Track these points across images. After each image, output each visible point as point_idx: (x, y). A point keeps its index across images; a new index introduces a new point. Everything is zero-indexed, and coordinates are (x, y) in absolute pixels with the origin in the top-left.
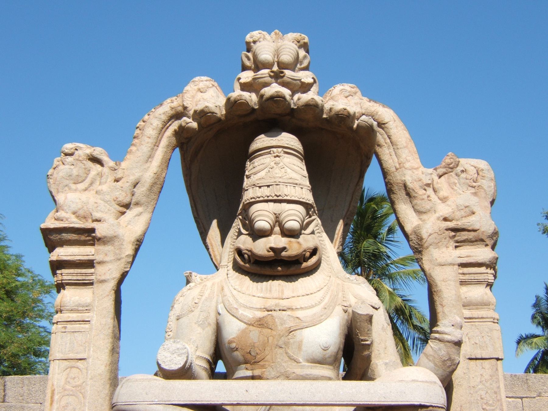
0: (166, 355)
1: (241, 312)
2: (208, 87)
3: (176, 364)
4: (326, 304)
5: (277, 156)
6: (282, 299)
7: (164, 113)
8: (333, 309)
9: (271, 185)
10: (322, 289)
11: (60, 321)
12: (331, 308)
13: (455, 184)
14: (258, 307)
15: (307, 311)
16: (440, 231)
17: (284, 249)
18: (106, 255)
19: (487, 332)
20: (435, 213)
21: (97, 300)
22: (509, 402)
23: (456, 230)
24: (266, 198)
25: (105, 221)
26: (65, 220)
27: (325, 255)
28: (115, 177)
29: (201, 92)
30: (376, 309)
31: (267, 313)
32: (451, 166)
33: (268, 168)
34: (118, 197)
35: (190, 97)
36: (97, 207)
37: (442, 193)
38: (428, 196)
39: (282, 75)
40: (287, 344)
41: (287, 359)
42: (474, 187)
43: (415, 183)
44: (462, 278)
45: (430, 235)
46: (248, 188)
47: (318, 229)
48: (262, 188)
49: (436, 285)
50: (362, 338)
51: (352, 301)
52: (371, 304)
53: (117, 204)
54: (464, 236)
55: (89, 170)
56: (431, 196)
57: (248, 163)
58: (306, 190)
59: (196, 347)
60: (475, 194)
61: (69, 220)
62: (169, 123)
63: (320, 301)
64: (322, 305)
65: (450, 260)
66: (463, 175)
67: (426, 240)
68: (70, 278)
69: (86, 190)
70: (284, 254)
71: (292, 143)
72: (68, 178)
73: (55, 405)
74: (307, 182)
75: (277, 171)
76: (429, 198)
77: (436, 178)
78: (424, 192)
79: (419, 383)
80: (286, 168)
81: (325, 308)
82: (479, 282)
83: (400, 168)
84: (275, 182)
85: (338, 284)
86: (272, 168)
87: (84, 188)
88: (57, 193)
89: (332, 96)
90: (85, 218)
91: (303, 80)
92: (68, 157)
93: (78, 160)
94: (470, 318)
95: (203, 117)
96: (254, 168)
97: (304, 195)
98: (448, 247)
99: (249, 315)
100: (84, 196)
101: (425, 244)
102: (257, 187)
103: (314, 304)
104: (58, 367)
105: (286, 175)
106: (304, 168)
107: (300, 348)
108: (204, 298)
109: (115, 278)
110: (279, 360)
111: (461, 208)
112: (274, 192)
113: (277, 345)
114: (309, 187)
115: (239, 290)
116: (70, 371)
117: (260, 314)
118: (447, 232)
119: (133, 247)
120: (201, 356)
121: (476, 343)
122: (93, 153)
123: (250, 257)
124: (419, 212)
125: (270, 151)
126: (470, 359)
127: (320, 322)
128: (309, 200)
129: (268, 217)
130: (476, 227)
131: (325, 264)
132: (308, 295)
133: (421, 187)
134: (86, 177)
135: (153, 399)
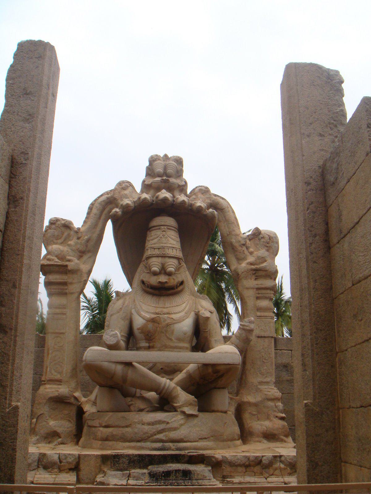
0: (108, 337)
1: (143, 313)
2: (128, 187)
3: (113, 342)
4: (186, 311)
5: (164, 231)
7: (103, 201)
8: (191, 313)
9: (160, 248)
12: (189, 313)
13: (258, 244)
15: (177, 314)
17: (166, 282)
18: (73, 279)
19: (268, 324)
20: (246, 259)
22: (285, 353)
23: (256, 270)
24: (157, 255)
27: (187, 284)
29: (124, 189)
30: (211, 312)
31: (155, 316)
32: (256, 234)
34: (79, 247)
36: (68, 253)
37: (251, 250)
38: (244, 251)
39: (168, 181)
40: (166, 331)
42: (267, 247)
44: (257, 295)
45: (242, 273)
49: (244, 299)
51: (200, 308)
53: (79, 252)
54: (260, 273)
55: (64, 232)
57: (148, 233)
60: (268, 251)
61: (54, 260)
62: (106, 206)
64: (186, 310)
65: (252, 286)
66: (263, 240)
69: (62, 243)
70: (166, 285)
71: (172, 224)
73: (50, 356)
74: (178, 245)
75: (164, 239)
77: (248, 241)
79: (228, 354)
80: (168, 238)
81: (186, 313)
82: (266, 298)
83: (229, 234)
84: (162, 246)
85: (193, 299)
87: (61, 242)
88: (47, 245)
90: (62, 259)
91: (179, 184)
94: (260, 316)
96: (151, 236)
99: (148, 316)
100: (61, 247)
103: (180, 311)
106: (178, 236)
107: (173, 333)
108: (125, 306)
109: (78, 292)
111: (260, 258)
114: (180, 249)
115: (142, 302)
117: (153, 316)
118: (251, 272)
119: (87, 276)
125: (160, 228)
126: (258, 337)
127: (184, 320)
129: (158, 265)
130: (267, 269)
131: (187, 288)
132: (177, 306)
133: (240, 246)
134: (62, 237)
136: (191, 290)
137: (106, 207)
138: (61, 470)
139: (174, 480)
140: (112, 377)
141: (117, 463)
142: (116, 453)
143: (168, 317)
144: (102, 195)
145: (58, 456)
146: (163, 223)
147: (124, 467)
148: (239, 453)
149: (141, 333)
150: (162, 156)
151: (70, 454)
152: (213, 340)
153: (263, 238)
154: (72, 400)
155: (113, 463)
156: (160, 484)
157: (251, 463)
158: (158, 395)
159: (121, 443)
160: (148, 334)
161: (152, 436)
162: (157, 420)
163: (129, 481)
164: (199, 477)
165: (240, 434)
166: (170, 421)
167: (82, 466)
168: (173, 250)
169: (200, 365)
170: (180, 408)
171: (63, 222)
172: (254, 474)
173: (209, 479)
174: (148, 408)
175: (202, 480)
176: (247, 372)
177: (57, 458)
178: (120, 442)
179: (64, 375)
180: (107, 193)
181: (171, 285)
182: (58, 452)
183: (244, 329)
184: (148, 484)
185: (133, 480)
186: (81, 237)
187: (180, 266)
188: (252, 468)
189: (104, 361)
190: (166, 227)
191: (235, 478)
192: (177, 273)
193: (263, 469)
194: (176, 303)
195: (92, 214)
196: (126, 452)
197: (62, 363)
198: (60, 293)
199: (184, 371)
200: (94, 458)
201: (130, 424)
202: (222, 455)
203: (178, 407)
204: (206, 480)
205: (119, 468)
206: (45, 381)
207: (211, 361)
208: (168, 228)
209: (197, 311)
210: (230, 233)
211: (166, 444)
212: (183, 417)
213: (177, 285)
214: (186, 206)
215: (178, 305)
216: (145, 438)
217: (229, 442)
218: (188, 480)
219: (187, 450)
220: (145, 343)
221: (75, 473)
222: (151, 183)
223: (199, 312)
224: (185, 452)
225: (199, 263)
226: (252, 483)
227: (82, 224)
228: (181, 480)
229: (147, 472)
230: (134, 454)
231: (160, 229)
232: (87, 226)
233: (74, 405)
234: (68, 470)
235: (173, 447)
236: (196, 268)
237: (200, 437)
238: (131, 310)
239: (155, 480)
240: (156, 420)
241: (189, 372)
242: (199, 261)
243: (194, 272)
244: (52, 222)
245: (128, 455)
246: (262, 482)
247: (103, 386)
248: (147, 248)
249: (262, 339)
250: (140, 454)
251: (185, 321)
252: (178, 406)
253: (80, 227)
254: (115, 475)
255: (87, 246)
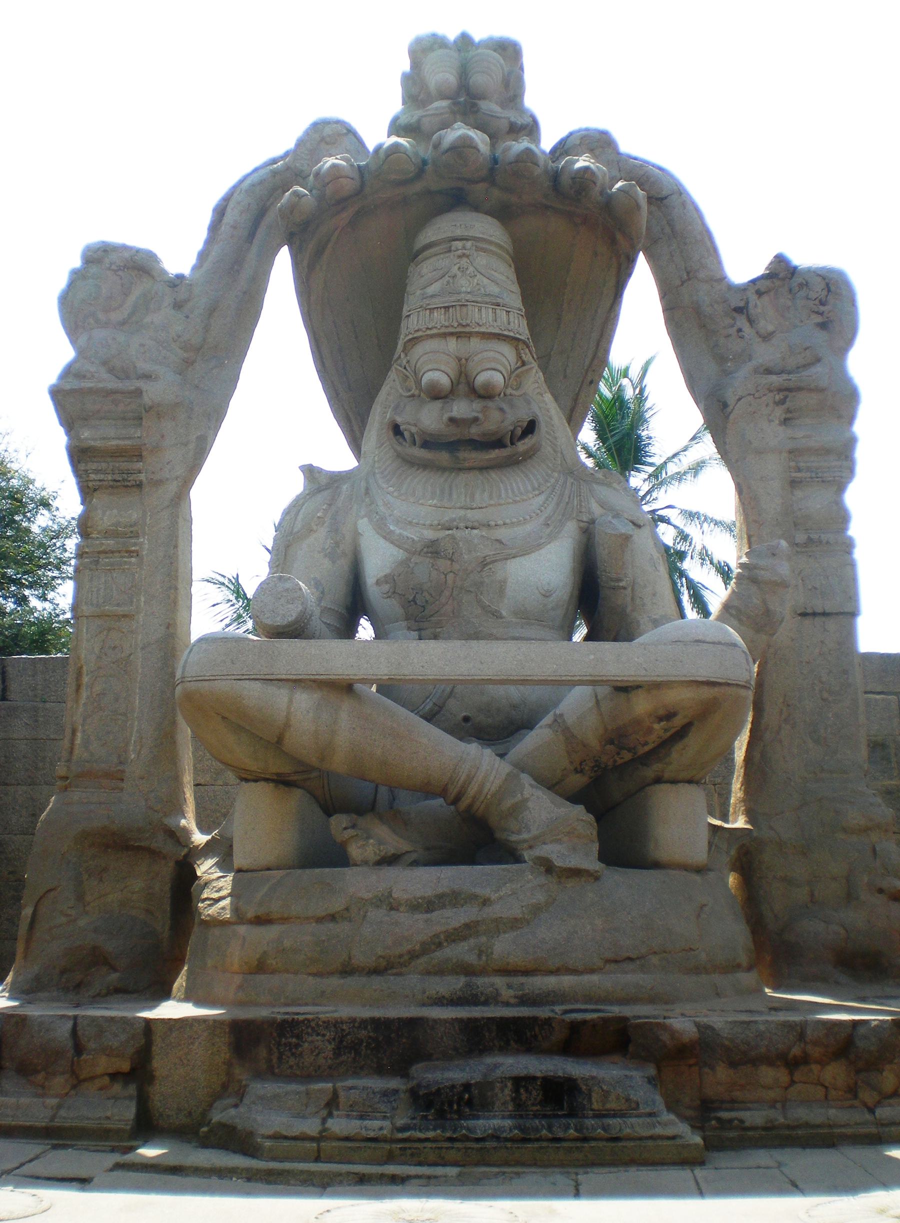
2: (339, 135)
4: (549, 518)
5: (464, 255)
6: (472, 509)
9: (453, 306)
10: (543, 492)
11: (87, 550)
14: (428, 522)
16: (758, 391)
17: (476, 420)
20: (750, 360)
21: (150, 515)
24: (443, 330)
25: (157, 378)
26: (88, 375)
28: (175, 299)
29: (327, 143)
30: (639, 526)
33: (447, 276)
35: (306, 152)
37: (765, 325)
38: (740, 330)
39: (475, 109)
41: (480, 611)
42: (822, 314)
43: (716, 306)
44: (794, 475)
45: (739, 399)
46: (410, 313)
47: (537, 388)
48: (435, 311)
50: (614, 576)
52: (630, 518)
56: (743, 329)
57: (410, 269)
58: (516, 315)
59: (323, 593)
63: (539, 511)
67: (731, 407)
68: (102, 477)
70: (474, 432)
72: (92, 302)
73: (84, 694)
76: (740, 334)
77: (753, 298)
78: (732, 322)
79: (705, 646)
81: (548, 524)
83: (689, 279)
84: (459, 301)
86: (454, 277)
89: (566, 147)
91: (513, 119)
92: (90, 264)
93: (109, 269)
95: (330, 185)
96: (422, 276)
97: (512, 324)
98: (773, 421)
101: (732, 414)
102: (426, 309)
104: (87, 629)
105: (479, 290)
106: (513, 277)
107: (501, 590)
109: (177, 478)
110: (465, 613)
112: (457, 319)
113: (461, 588)
114: (520, 310)
115: (395, 494)
116: (107, 636)
117: (430, 535)
118: (771, 394)
120: (330, 609)
121: (815, 588)
122: (136, 257)
123: (416, 436)
124: (721, 360)
125: (450, 247)
126: (804, 615)
127: (539, 547)
128: (520, 332)
131: (549, 449)
132: (515, 502)
135: (244, 672)
136: (562, 453)
137: (268, 203)
138: (82, 1077)
139: (510, 1117)
140: (280, 740)
141: (293, 1054)
142: (287, 1013)
143: (482, 536)
144: (256, 170)
145: (70, 1024)
146: (458, 233)
147: (319, 1067)
148: (760, 1013)
149: (388, 595)
150: (452, 35)
151: (112, 1019)
152: (643, 620)
153: (805, 285)
154: (159, 842)
155: (276, 1054)
156: (455, 1131)
157: (809, 1048)
158: (452, 807)
159: (311, 978)
160: (415, 597)
161: (427, 948)
162: (447, 890)
163: (330, 1123)
164: (608, 1106)
165: (753, 947)
166: (494, 897)
167: (160, 1064)
168: (498, 311)
169: (603, 691)
170: (531, 847)
171: (126, 255)
172: (820, 1092)
173: (650, 1115)
174: (415, 851)
175: (623, 1116)
176: (768, 736)
177: (67, 1035)
178: (310, 974)
179: (133, 756)
180: (274, 161)
181: (491, 428)
182: (71, 1013)
183: (754, 581)
184: (406, 1135)
185: (348, 1116)
186: (189, 300)
187: (525, 368)
188: (815, 1068)
189: (248, 679)
190: (469, 244)
191: (749, 1109)
192: (514, 392)
193: (858, 1071)
194: (513, 492)
195: (223, 228)
196: (326, 1013)
197: (125, 714)
198: (119, 484)
199: (548, 719)
200: (205, 1034)
201: (347, 909)
202: (697, 1019)
203: (525, 845)
204: (638, 1116)
205: (298, 1072)
206: (67, 778)
207: (643, 673)
208: (476, 247)
209: (585, 519)
210: (690, 275)
211: (481, 981)
212: (542, 880)
213: (512, 432)
214: (538, 171)
215: (518, 499)
216: (402, 960)
217: (717, 978)
218: (564, 1116)
219: (562, 1004)
220: (405, 631)
221: (132, 1089)
222: (419, 121)
223: (592, 522)
224: (553, 1011)
225: (589, 379)
226: (819, 1126)
227: (192, 260)
228: (535, 1116)
229: (403, 1087)
230: (353, 1020)
231: (450, 251)
232: (207, 265)
233: (165, 858)
234: (106, 1080)
235: (507, 994)
236: (578, 394)
237: (609, 955)
238: (355, 525)
239: (435, 1119)
240: (440, 890)
241: (564, 721)
242: (587, 371)
243: (572, 410)
244: (90, 254)
245: (336, 1024)
246: (856, 1124)
247: (256, 781)
248: (405, 312)
249: (818, 620)
250: (379, 1019)
251: (543, 551)
252: (525, 841)
253: (186, 271)
254: (276, 1097)
255: (207, 329)
